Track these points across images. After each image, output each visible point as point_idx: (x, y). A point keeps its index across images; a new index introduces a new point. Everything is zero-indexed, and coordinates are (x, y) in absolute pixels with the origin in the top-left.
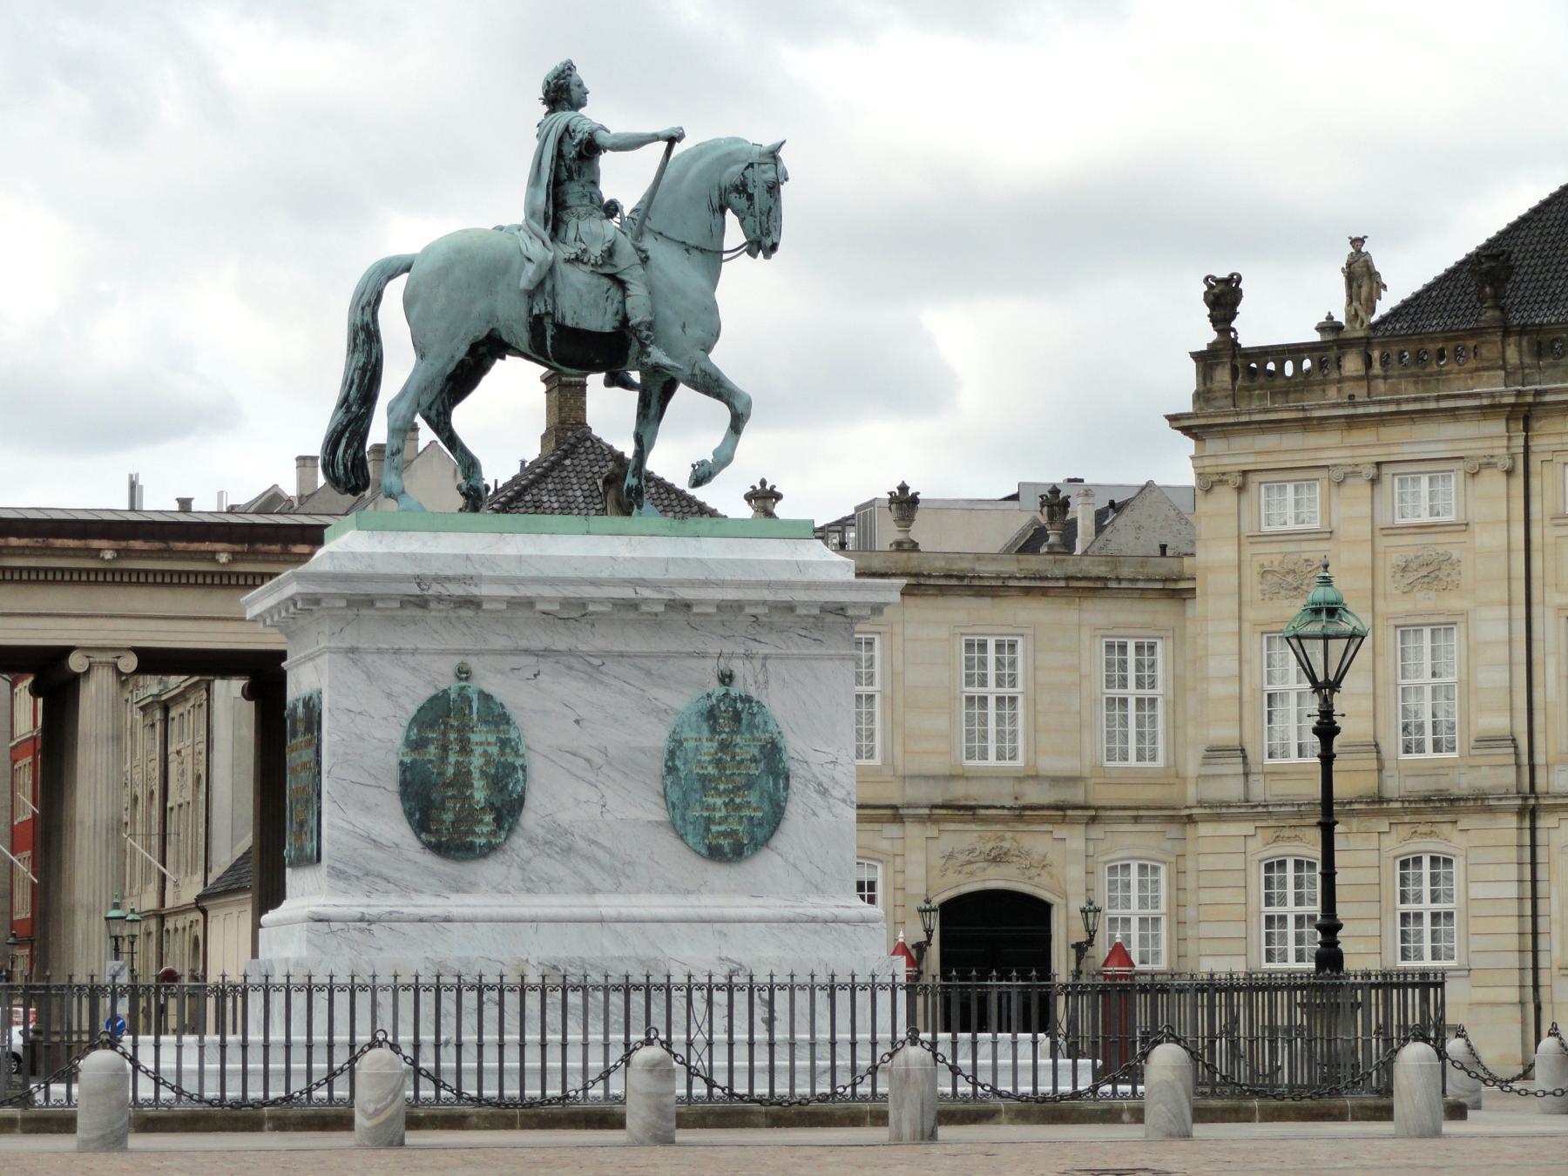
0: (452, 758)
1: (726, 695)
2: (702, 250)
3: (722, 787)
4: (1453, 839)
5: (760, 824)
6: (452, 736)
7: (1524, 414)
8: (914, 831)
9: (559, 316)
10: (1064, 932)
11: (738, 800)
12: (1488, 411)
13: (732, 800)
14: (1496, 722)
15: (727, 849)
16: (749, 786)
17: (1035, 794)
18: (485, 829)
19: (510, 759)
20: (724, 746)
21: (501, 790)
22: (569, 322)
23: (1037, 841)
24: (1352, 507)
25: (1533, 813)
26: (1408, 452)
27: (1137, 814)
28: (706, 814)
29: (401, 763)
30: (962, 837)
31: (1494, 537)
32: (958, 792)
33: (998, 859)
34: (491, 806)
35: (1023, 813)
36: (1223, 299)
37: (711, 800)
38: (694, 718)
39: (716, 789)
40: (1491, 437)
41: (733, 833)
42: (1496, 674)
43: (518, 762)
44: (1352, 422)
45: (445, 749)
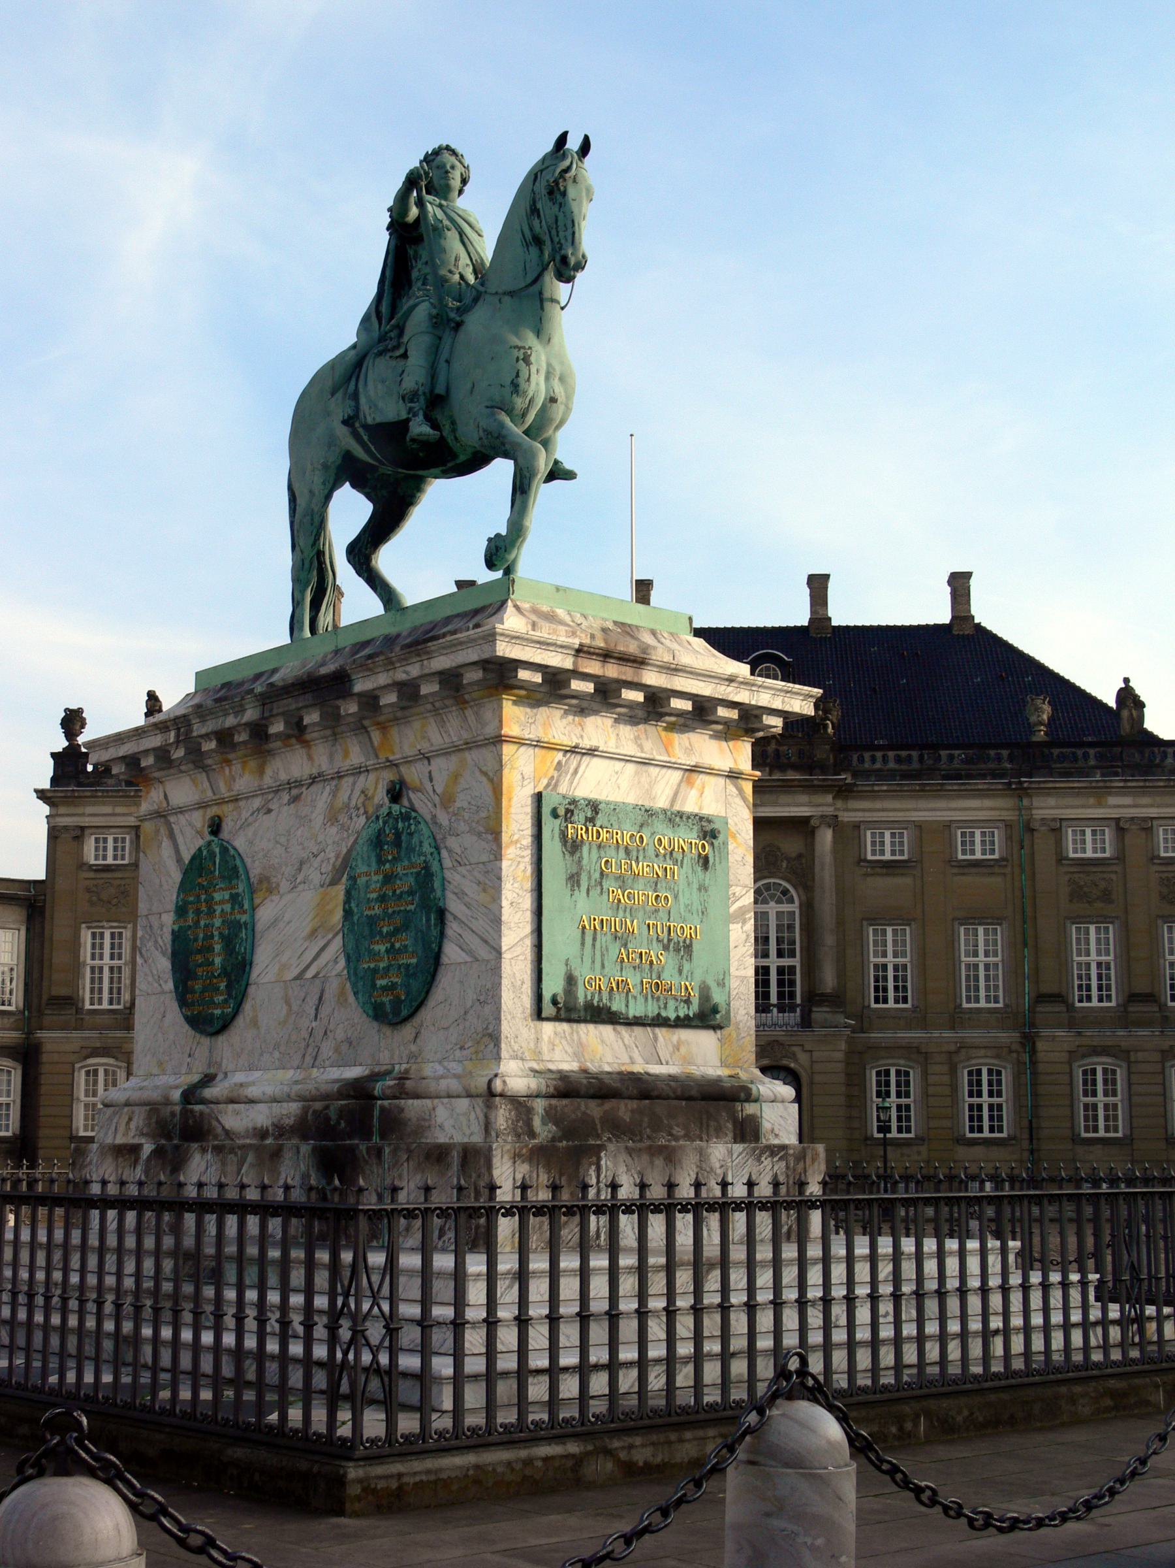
0: (202, 923)
1: (389, 814)
2: (511, 294)
3: (385, 930)
5: (414, 974)
6: (203, 897)
9: (361, 416)
11: (397, 945)
13: (393, 946)
15: (388, 1008)
16: (405, 927)
18: (221, 998)
19: (238, 917)
20: (389, 879)
21: (230, 955)
22: (369, 421)
28: (372, 965)
29: (173, 932)
34: (225, 973)
37: (376, 947)
38: (365, 849)
39: (380, 933)
41: (392, 987)
43: (244, 918)
45: (198, 912)
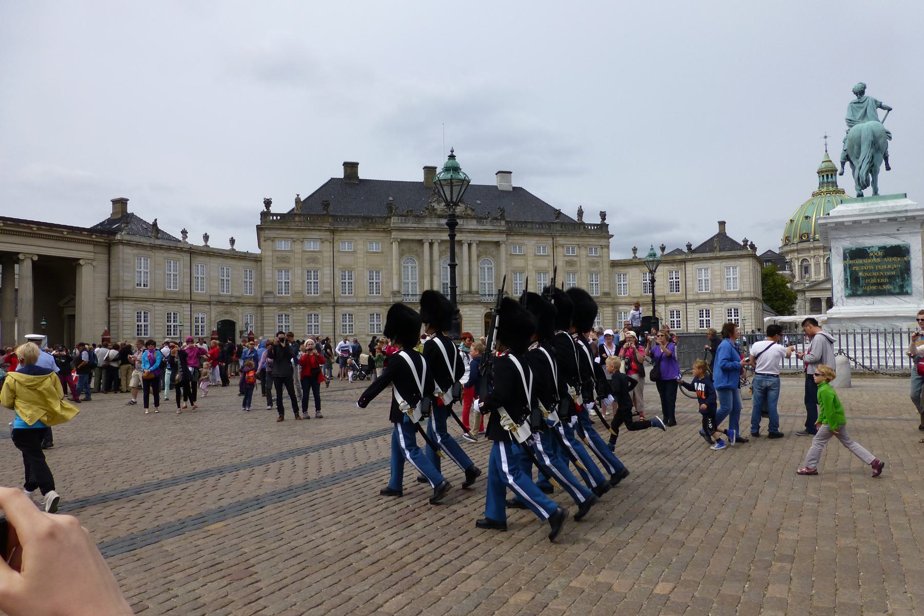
4: (318, 311)
7: (333, 232)
8: (212, 307)
10: (239, 328)
12: (326, 230)
14: (327, 289)
17: (234, 300)
23: (234, 310)
24: (298, 247)
25: (334, 306)
26: (310, 236)
27: (250, 304)
30: (221, 308)
31: (327, 254)
32: (220, 299)
33: (226, 313)
35: (232, 304)
36: (268, 203)
40: (327, 235)
42: (327, 280)
44: (298, 230)
